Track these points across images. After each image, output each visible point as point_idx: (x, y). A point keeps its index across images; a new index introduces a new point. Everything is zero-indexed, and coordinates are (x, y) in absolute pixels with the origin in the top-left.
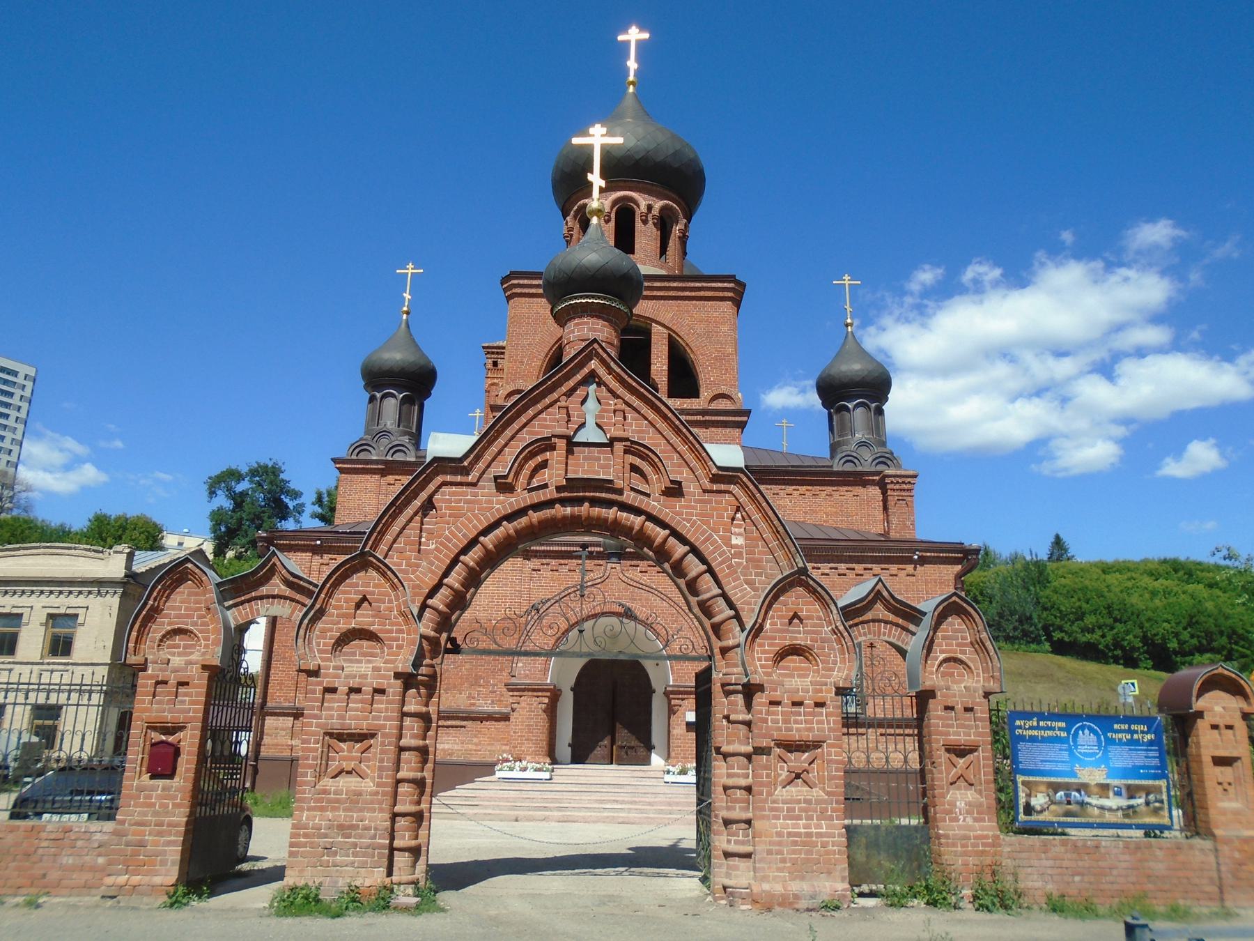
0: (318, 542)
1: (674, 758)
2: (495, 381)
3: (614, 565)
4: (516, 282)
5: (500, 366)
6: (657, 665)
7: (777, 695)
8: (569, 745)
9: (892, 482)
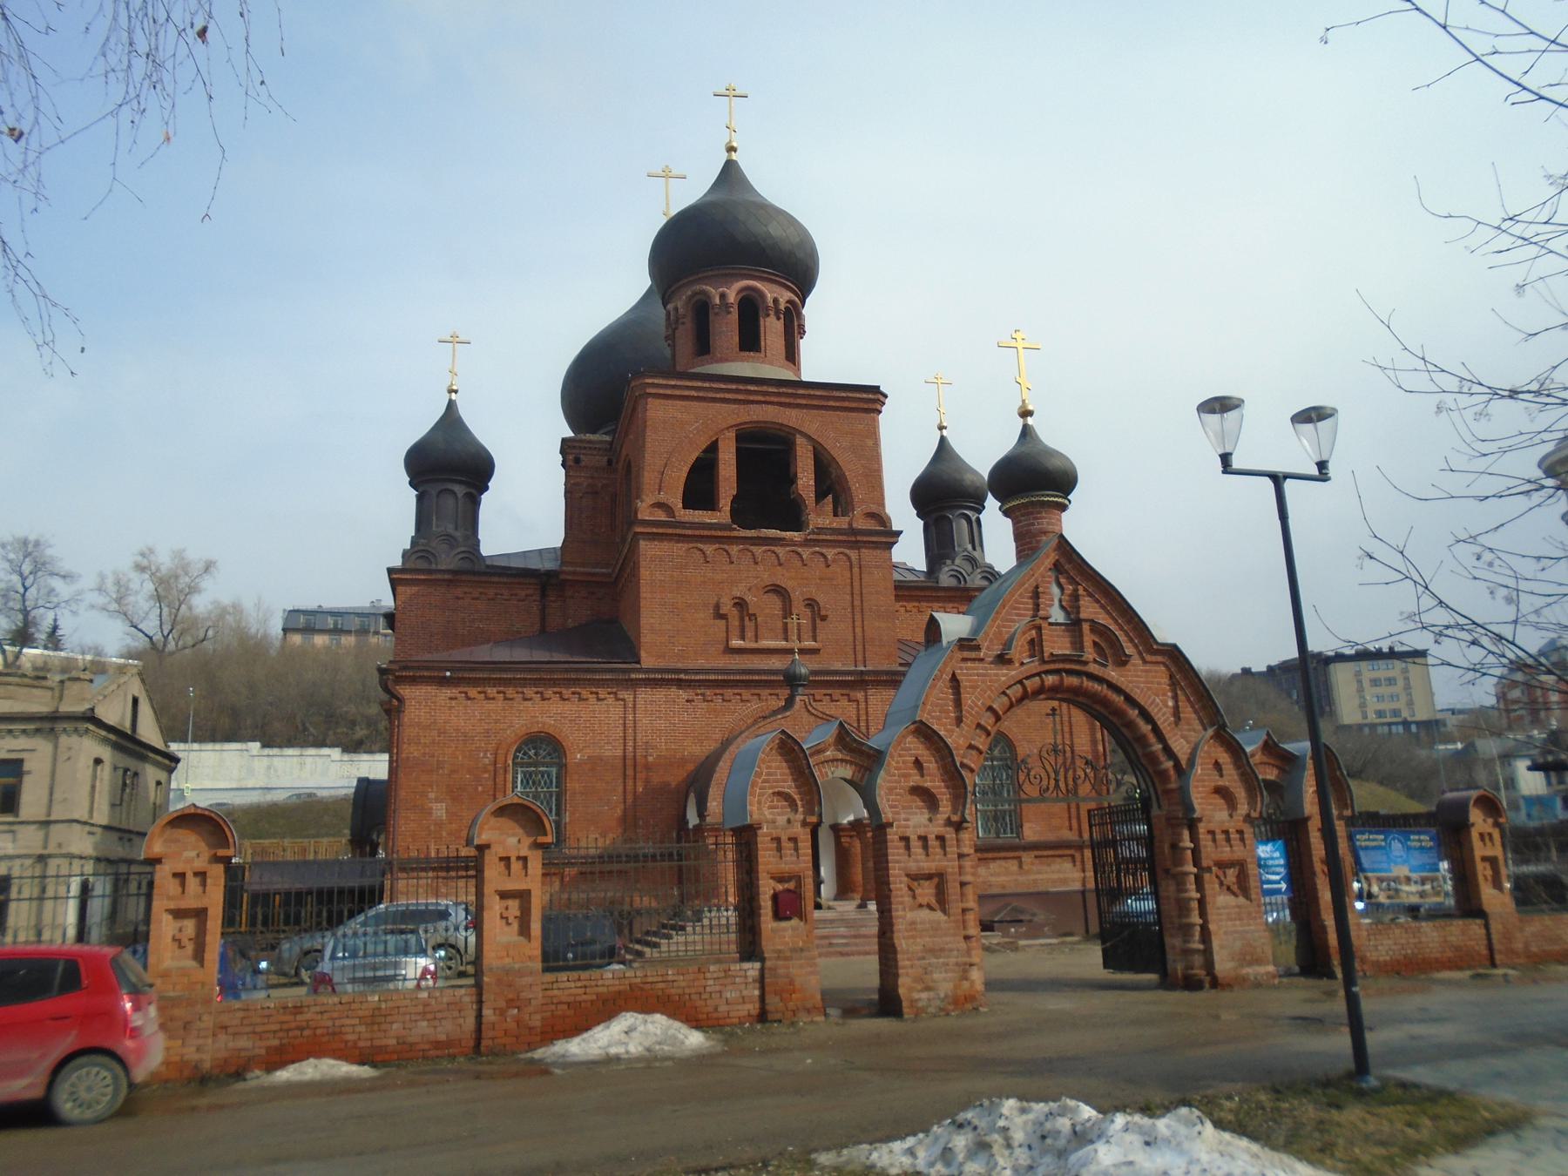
0: (448, 674)
2: (578, 480)
3: (802, 698)
4: (650, 381)
5: (583, 464)
7: (1212, 826)
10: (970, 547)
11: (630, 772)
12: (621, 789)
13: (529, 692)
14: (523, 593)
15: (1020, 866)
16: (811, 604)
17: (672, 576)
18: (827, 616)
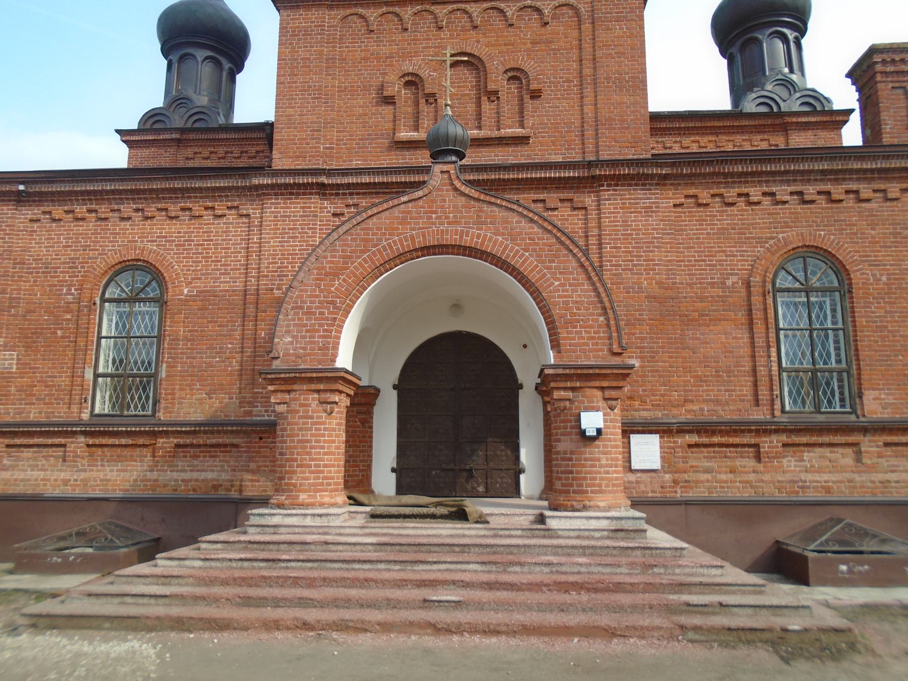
0: (21, 187)
1: (561, 492)
3: (445, 168)
6: (525, 346)
8: (393, 470)
9: (884, 62)
10: (786, 70)
11: (251, 309)
12: (237, 334)
13: (127, 209)
14: (253, 150)
15: (858, 460)
16: (516, 75)
17: (321, 53)
18: (539, 91)
